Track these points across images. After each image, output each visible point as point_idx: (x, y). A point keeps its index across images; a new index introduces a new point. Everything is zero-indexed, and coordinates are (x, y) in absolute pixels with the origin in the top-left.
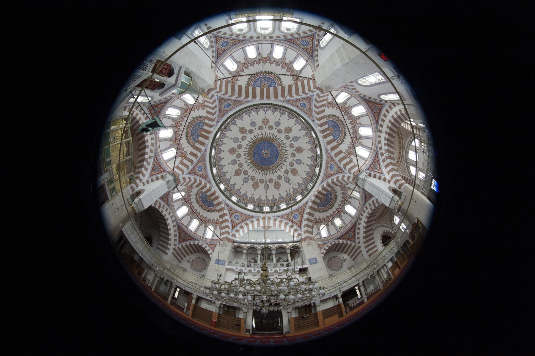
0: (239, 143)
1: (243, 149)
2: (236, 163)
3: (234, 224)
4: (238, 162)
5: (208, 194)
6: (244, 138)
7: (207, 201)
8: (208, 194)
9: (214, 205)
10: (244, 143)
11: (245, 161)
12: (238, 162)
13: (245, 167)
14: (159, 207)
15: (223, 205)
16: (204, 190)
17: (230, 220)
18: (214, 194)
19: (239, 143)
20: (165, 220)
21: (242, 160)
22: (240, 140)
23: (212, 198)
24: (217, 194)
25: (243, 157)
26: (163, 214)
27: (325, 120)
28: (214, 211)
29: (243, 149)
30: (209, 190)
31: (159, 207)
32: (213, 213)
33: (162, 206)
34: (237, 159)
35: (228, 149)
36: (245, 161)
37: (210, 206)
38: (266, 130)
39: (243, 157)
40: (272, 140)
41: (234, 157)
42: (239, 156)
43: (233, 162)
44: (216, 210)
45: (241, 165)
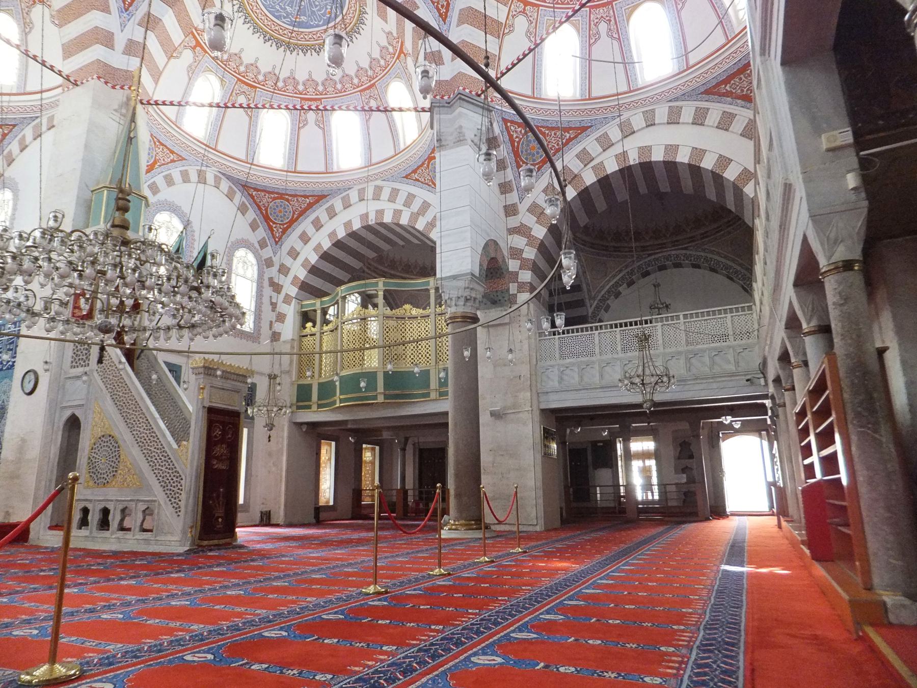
20: (647, 167)
26: (612, 167)
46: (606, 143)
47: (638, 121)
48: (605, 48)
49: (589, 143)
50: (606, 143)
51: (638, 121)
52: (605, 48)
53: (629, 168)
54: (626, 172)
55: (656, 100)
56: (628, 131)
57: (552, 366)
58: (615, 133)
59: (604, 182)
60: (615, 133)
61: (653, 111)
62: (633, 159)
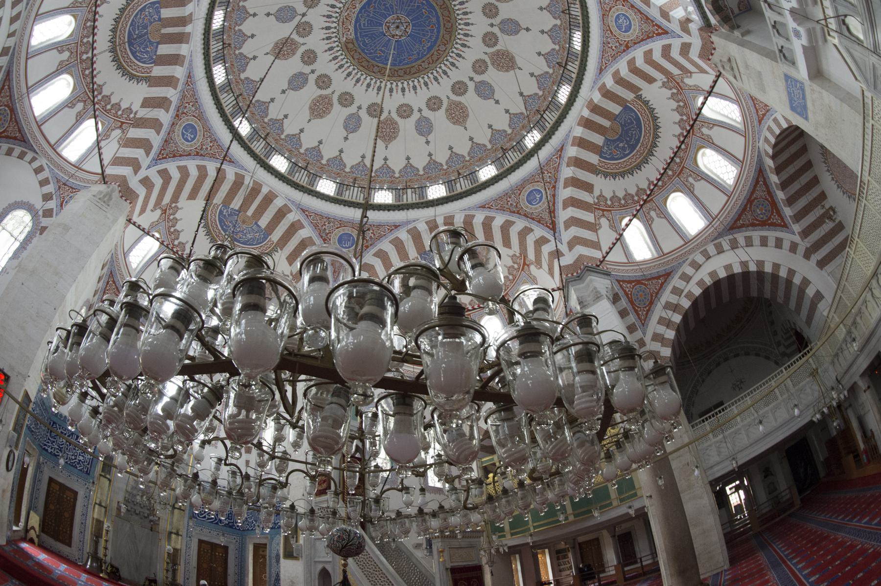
0: (426, 113)
1: (435, 90)
2: (482, 82)
3: (646, 28)
4: (478, 78)
5: (598, 139)
6: (405, 111)
7: (625, 134)
8: (598, 139)
9: (626, 108)
10: (417, 99)
11: (460, 63)
12: (478, 78)
13: (476, 50)
14: (675, 308)
15: (609, 81)
16: (593, 158)
17: (646, 48)
18: (587, 124)
19: (426, 113)
20: (717, 284)
21: (463, 71)
22: (416, 116)
23: (606, 123)
24: (586, 113)
25: (455, 76)
26: (698, 291)
27: (158, 71)
28: (646, 103)
29: (435, 90)
30: (582, 143)
31: (675, 308)
32: (654, 103)
33: (674, 299)
34: (471, 86)
35: (459, 128)
36: (460, 63)
37: (638, 119)
38: (340, 83)
39: (455, 76)
40: (348, 48)
41: (470, 99)
42: (459, 88)
43: (485, 91)
44: (639, 97)
45: (479, 67)
46: (687, 278)
47: (700, 259)
48: (659, 224)
49: (676, 281)
50: (687, 278)
51: (700, 259)
52: (659, 224)
53: (708, 288)
54: (706, 292)
55: (705, 242)
56: (697, 266)
57: (710, 446)
58: (689, 271)
59: (695, 303)
60: (689, 271)
61: (706, 250)
62: (709, 281)
